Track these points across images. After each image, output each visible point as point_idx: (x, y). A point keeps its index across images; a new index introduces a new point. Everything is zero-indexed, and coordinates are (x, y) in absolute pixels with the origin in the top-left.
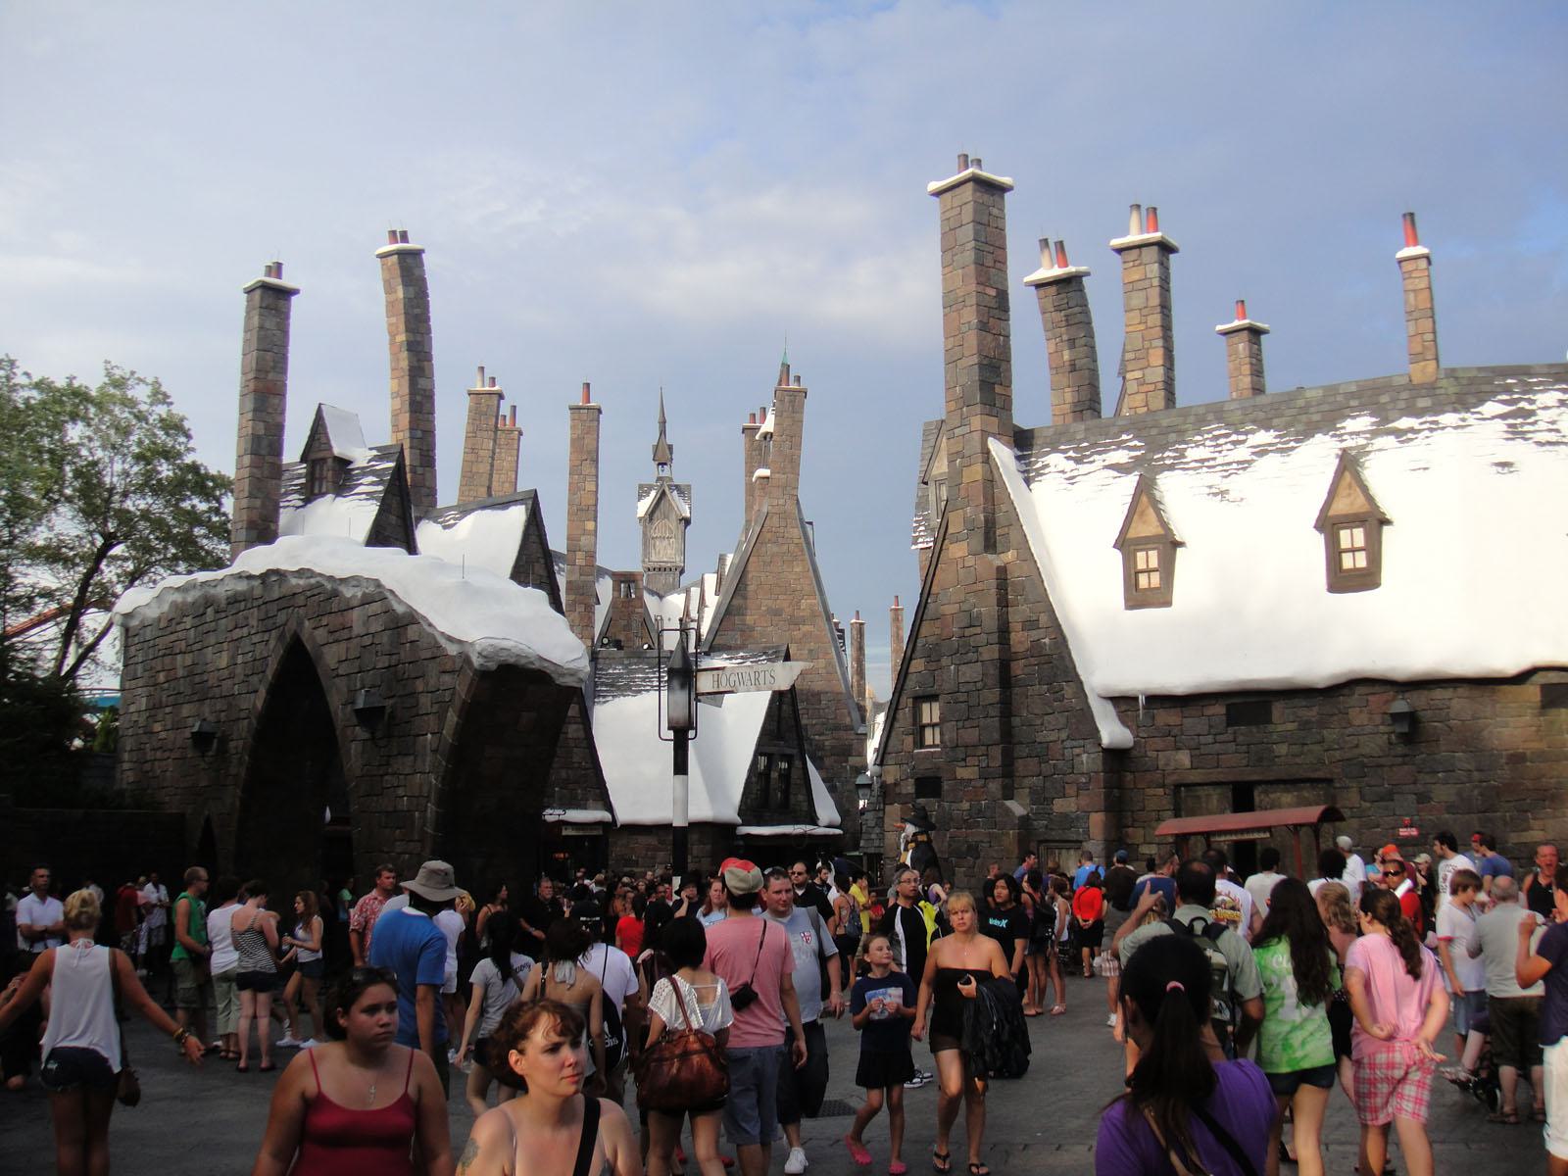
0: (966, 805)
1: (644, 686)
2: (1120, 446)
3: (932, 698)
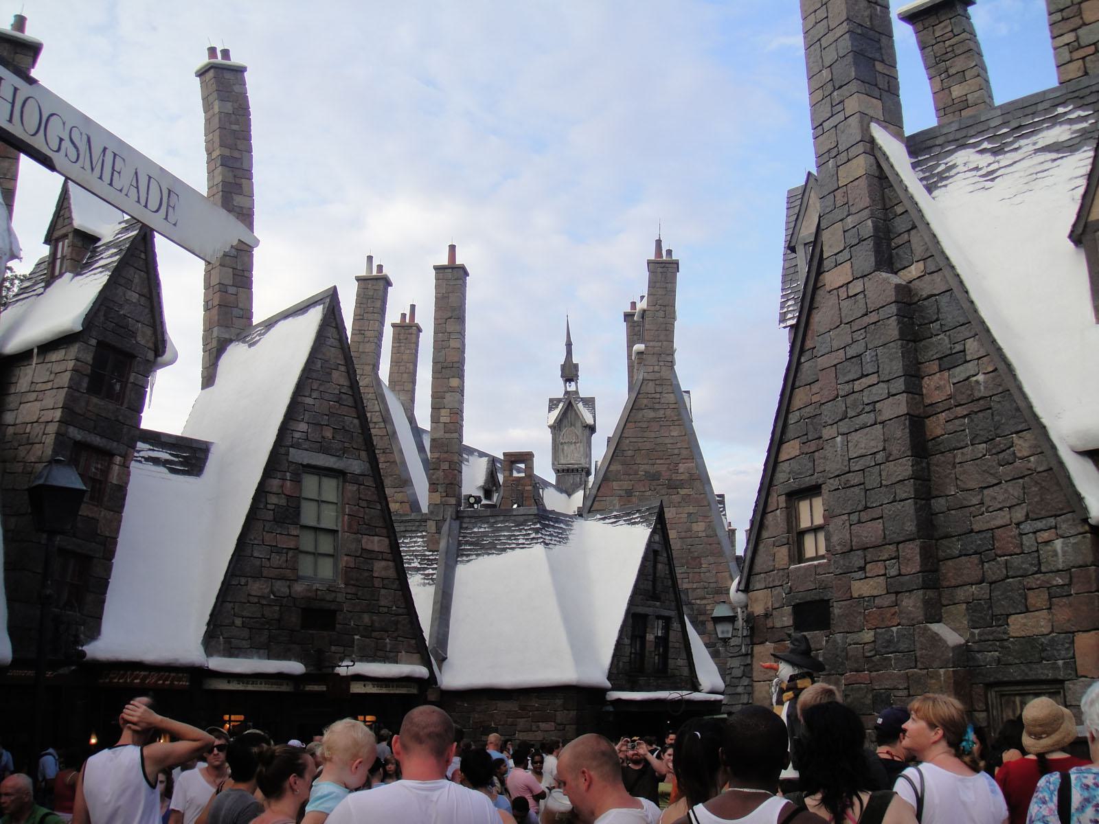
0: (868, 636)
1: (509, 544)
2: (1055, 121)
3: (812, 491)
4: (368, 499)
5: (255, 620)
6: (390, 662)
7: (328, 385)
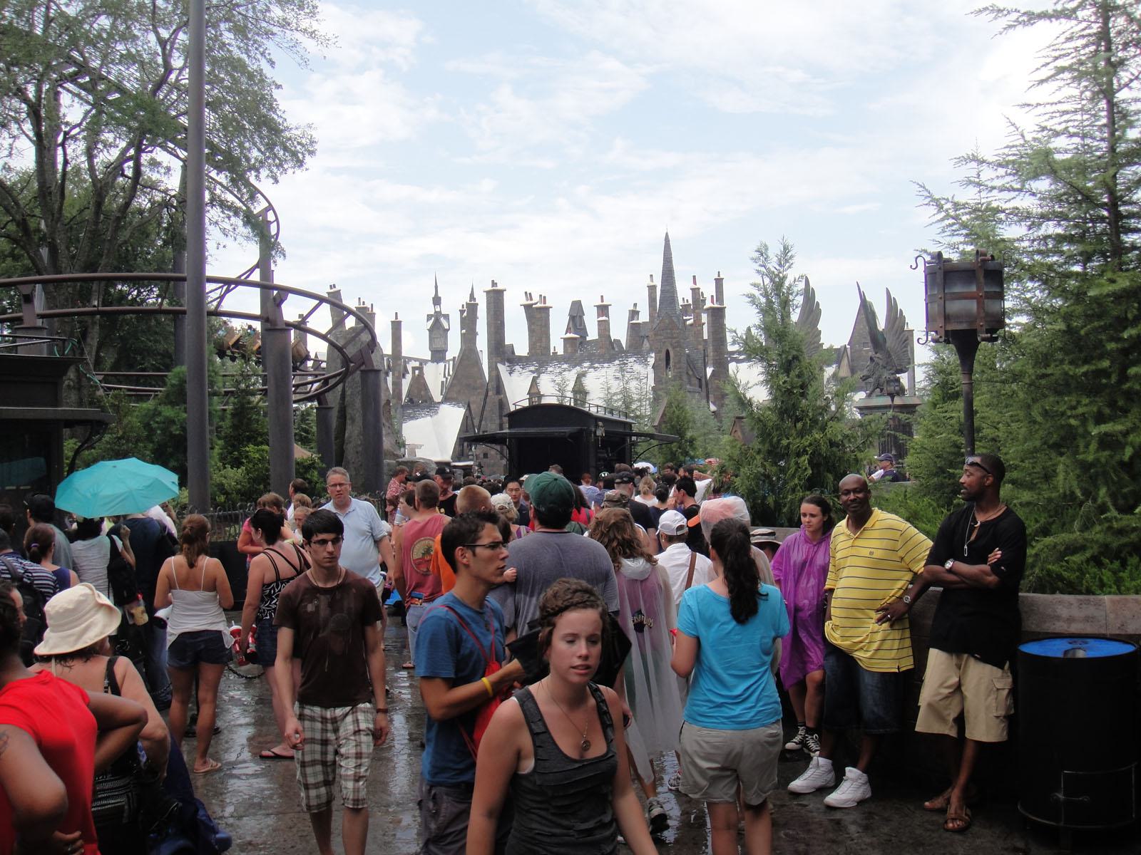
2: (533, 365)
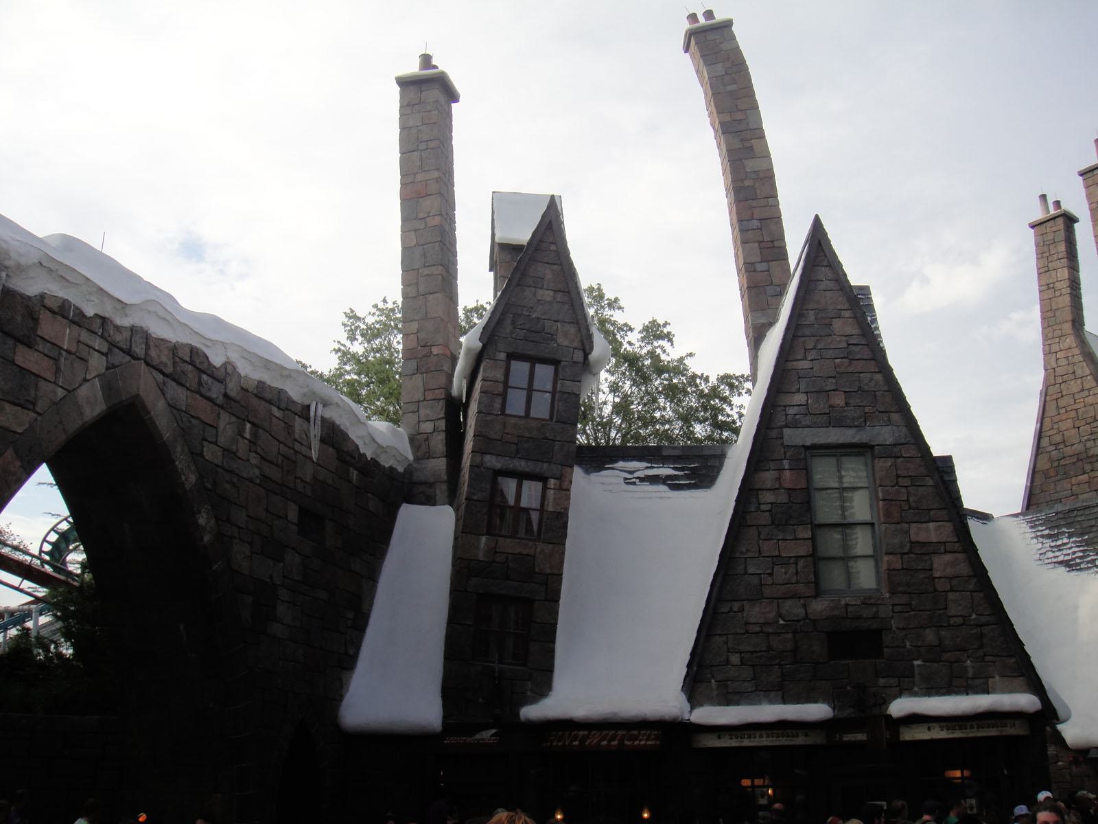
4: (910, 474)
5: (759, 654)
6: (977, 693)
7: (829, 339)
